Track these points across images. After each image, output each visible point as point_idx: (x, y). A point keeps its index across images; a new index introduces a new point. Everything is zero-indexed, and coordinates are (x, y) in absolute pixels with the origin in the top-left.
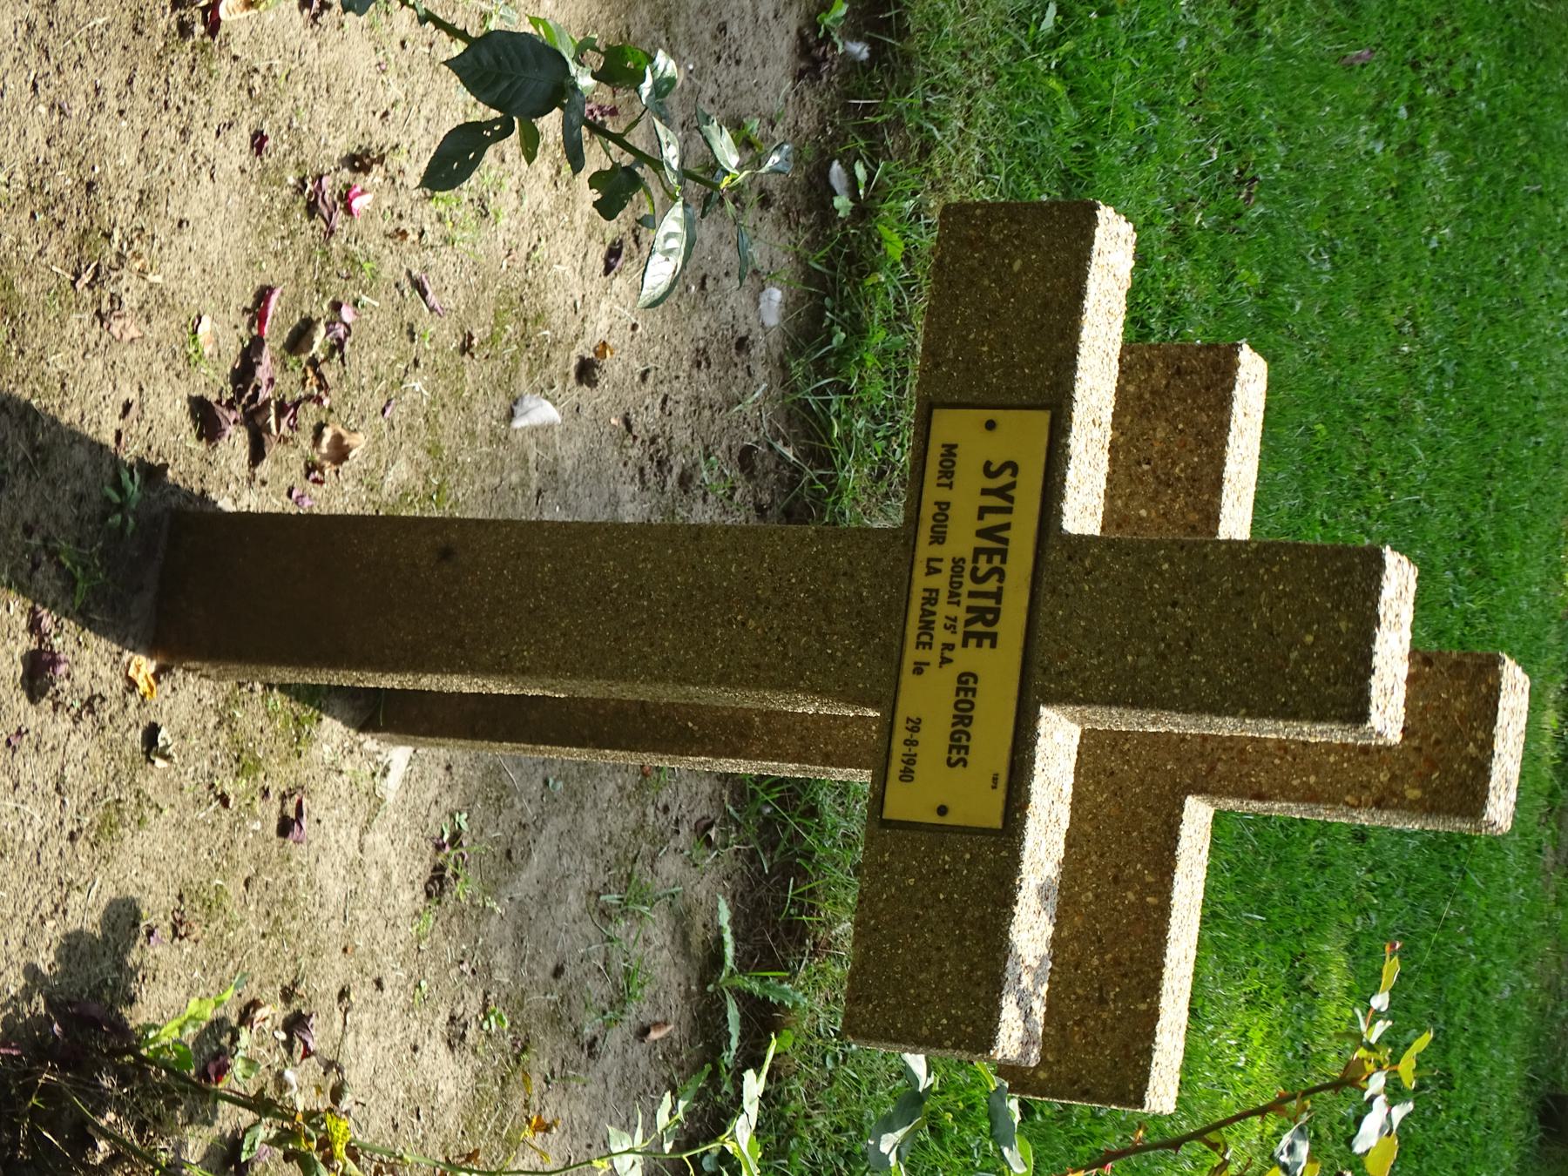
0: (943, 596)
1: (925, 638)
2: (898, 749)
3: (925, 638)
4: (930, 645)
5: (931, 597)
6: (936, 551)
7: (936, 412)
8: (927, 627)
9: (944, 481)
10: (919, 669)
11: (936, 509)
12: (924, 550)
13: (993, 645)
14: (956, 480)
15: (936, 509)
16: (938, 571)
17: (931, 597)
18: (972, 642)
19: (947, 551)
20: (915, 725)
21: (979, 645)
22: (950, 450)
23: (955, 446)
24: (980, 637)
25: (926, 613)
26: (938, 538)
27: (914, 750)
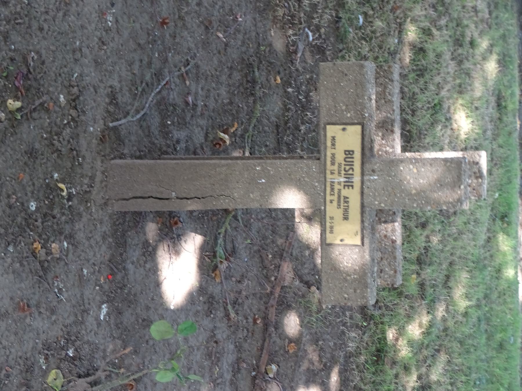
1: (332, 193)
3: (332, 193)
4: (334, 195)
6: (332, 168)
7: (328, 127)
8: (332, 189)
9: (333, 147)
10: (331, 202)
13: (353, 188)
14: (337, 147)
18: (346, 188)
20: (332, 218)
21: (348, 188)
23: (335, 137)
24: (348, 186)
26: (333, 164)
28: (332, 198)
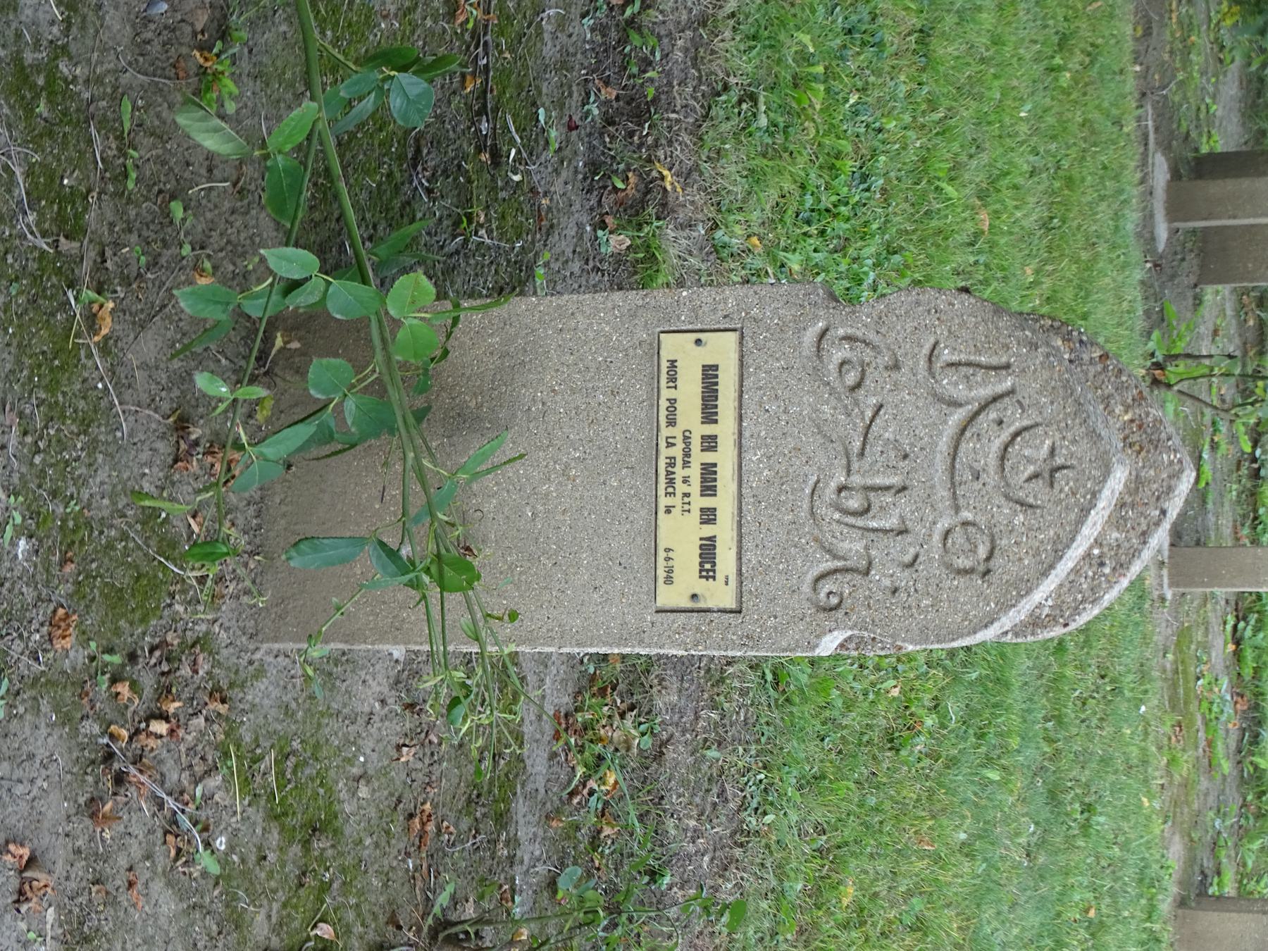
0: (679, 462)
1: (670, 490)
2: (661, 562)
3: (670, 490)
5: (671, 462)
8: (671, 482)
9: (671, 384)
11: (668, 404)
12: (665, 432)
15: (668, 404)
16: (674, 445)
17: (671, 462)
19: (677, 432)
22: (673, 363)
25: (668, 473)
26: (672, 423)
27: (671, 563)
28: (669, 501)
